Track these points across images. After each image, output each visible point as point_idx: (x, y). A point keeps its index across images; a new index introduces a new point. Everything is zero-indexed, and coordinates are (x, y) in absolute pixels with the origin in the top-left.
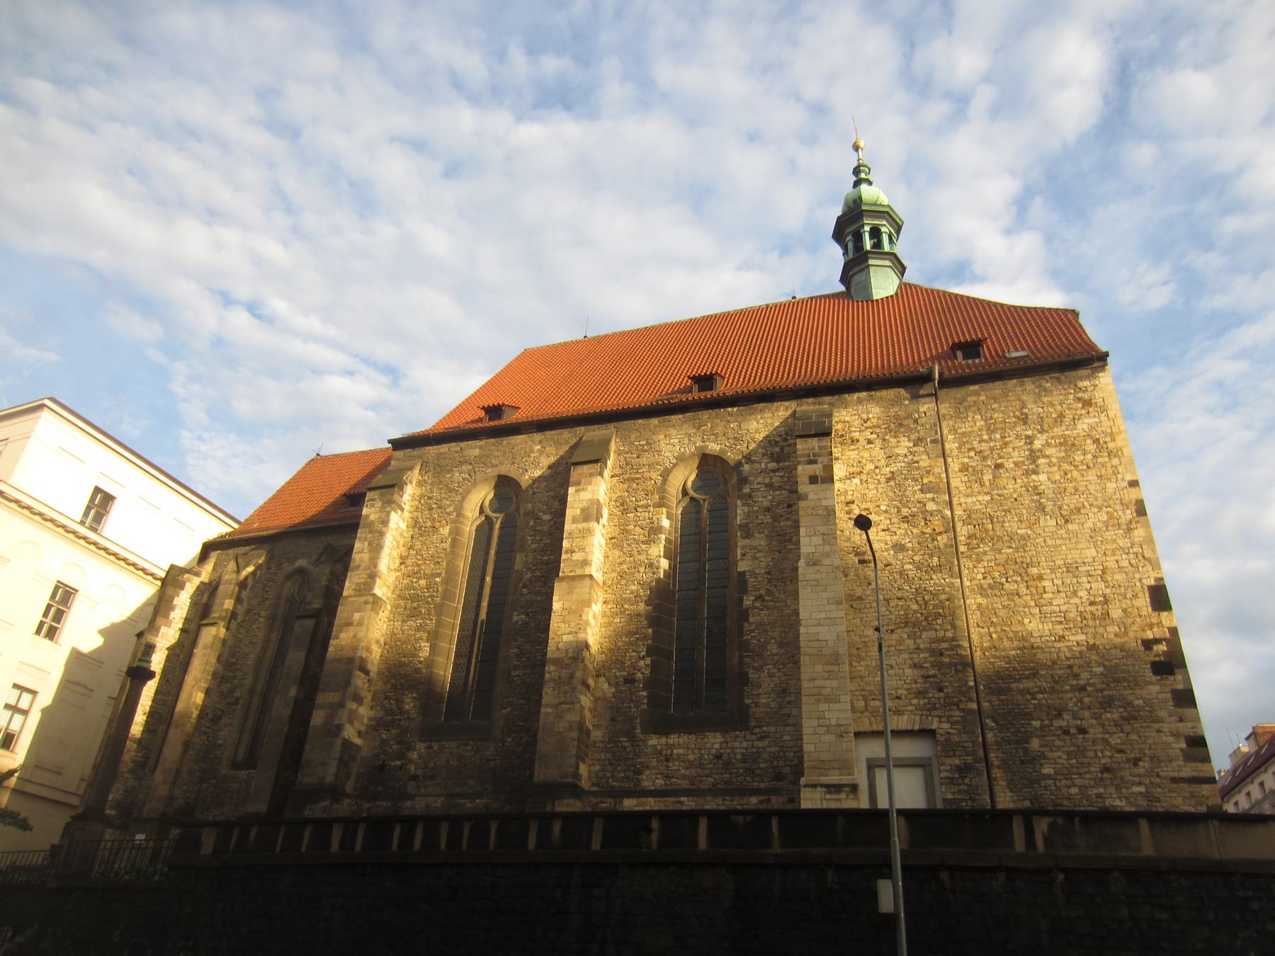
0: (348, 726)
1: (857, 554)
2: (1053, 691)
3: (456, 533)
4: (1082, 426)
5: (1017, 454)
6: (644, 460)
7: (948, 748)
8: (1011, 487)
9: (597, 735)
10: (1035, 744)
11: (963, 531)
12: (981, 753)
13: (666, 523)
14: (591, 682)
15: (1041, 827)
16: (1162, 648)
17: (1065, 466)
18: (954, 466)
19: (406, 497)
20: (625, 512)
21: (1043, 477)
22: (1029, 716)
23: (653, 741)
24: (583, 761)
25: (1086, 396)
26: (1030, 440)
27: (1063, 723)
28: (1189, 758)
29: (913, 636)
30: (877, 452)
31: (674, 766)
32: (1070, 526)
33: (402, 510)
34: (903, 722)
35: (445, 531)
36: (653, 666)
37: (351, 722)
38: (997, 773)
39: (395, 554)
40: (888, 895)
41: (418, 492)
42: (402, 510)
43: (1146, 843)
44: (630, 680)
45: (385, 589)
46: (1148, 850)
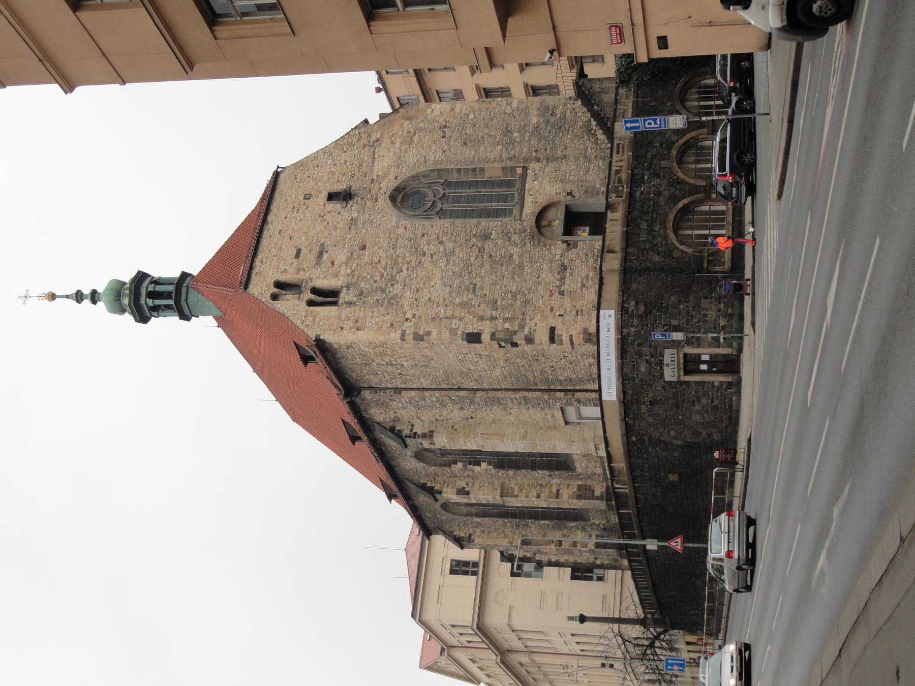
0: (589, 547)
1: (467, 419)
2: (532, 371)
3: (477, 515)
4: (367, 349)
5: (390, 368)
6: (423, 472)
7: (569, 404)
8: (412, 372)
9: (580, 483)
10: (560, 378)
11: (445, 386)
12: (570, 395)
13: (460, 465)
14: (554, 490)
15: (617, 486)
16: (503, 344)
17: (396, 356)
18: (404, 386)
19: (462, 534)
20: (456, 476)
21: (405, 364)
22: (547, 380)
23: (579, 470)
24: (593, 491)
25: (344, 347)
26: (378, 364)
27: (549, 372)
28: (561, 343)
29: (512, 408)
30: (401, 411)
31: (590, 466)
32: (435, 359)
33: (470, 535)
34: (559, 414)
35: (478, 520)
36: (542, 468)
37: (586, 546)
38: (577, 388)
39: (495, 534)
40: (652, 545)
41: (456, 528)
42: (470, 535)
43: (620, 464)
44: (551, 475)
45: (516, 537)
46: (623, 465)
